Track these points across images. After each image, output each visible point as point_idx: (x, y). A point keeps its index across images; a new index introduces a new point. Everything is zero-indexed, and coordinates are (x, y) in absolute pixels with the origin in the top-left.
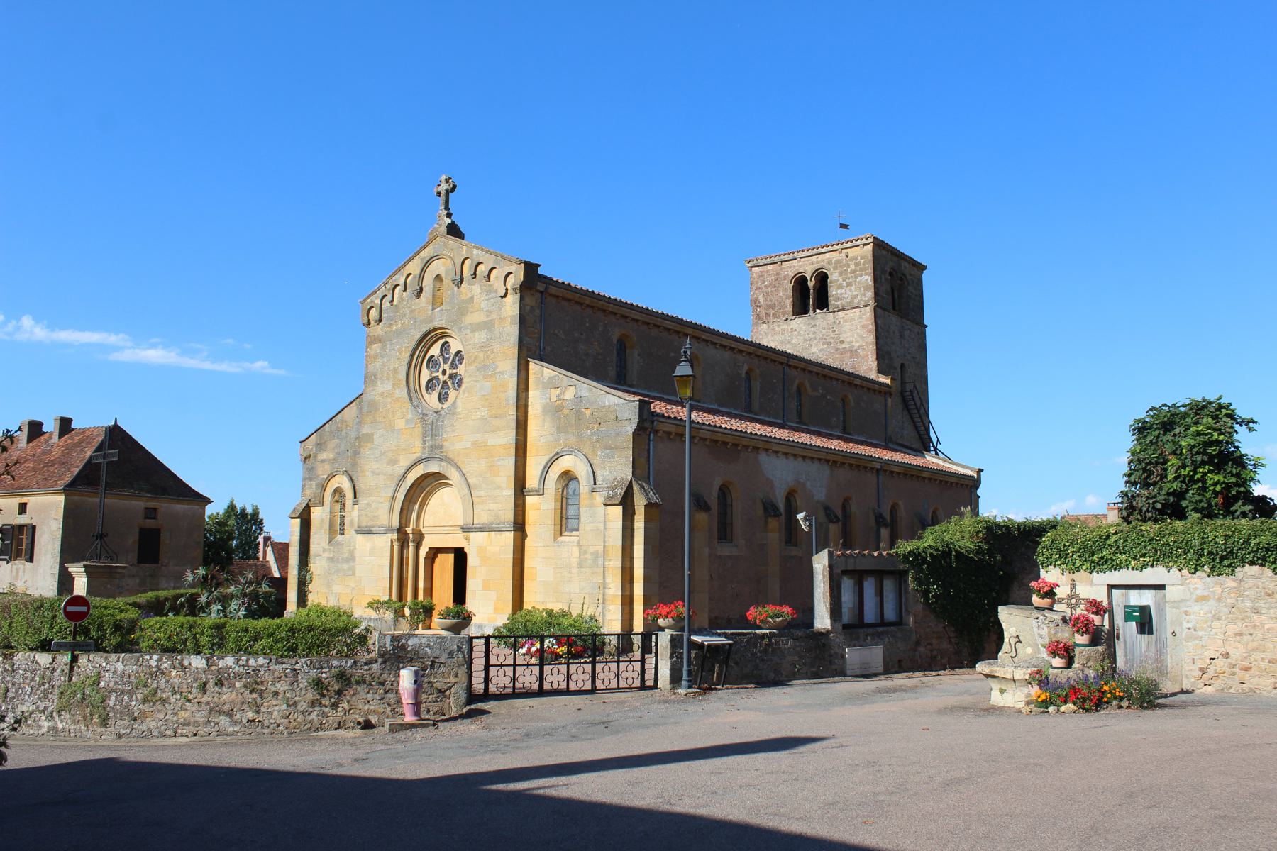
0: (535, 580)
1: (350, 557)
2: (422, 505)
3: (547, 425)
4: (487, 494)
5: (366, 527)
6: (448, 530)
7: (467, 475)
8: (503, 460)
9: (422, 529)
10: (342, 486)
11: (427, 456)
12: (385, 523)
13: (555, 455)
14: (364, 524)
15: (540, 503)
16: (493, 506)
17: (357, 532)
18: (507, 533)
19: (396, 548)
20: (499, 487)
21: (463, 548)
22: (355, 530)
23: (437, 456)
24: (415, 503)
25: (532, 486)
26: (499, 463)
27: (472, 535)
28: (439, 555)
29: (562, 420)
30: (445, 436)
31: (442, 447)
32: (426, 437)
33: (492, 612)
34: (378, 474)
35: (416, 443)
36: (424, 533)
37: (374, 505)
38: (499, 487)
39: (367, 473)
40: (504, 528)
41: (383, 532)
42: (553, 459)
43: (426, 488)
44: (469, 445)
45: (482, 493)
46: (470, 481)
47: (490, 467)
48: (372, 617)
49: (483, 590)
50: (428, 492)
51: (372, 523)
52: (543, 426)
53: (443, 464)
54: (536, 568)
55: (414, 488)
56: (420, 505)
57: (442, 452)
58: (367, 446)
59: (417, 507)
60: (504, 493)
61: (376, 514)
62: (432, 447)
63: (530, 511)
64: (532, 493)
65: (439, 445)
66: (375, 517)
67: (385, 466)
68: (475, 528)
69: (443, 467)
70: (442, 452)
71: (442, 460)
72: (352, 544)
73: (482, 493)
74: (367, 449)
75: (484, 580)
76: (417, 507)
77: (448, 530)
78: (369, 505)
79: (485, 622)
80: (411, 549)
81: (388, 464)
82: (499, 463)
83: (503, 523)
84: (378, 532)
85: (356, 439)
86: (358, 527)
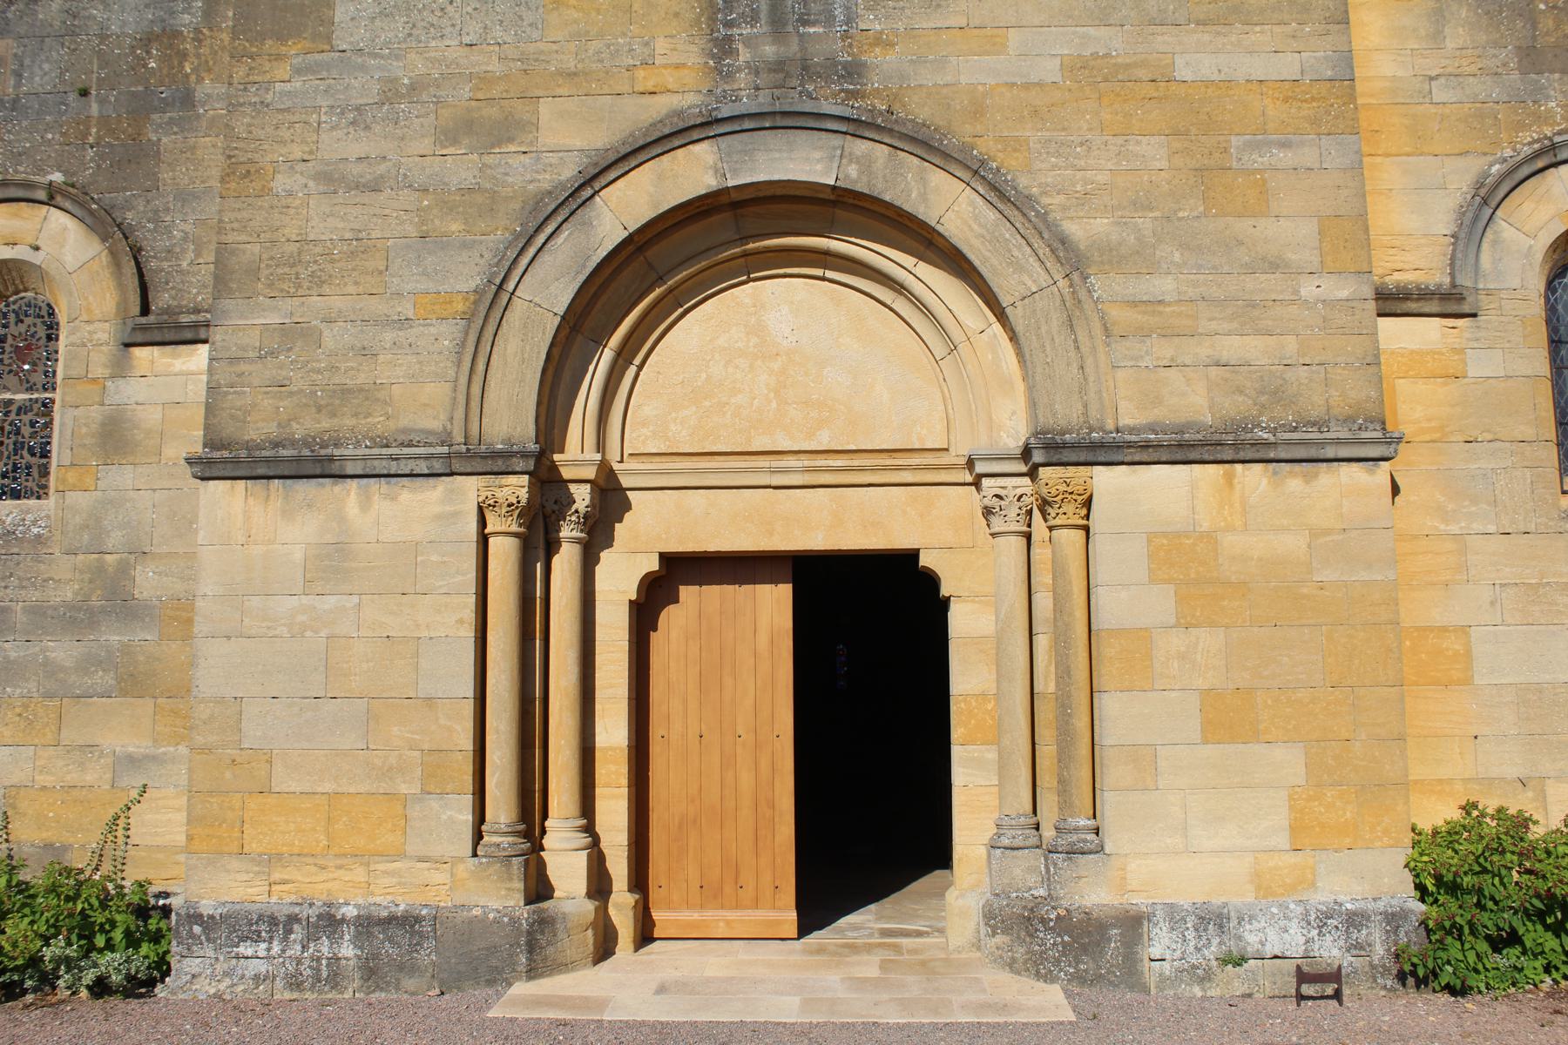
0: (1467, 681)
1: (96, 602)
2: (624, 356)
3: (1457, 36)
4: (1191, 292)
5: (276, 445)
6: (808, 470)
7: (1053, 201)
8: (1284, 145)
9: (616, 466)
10: (36, 258)
11: (746, 104)
12: (436, 425)
13: (1537, 155)
14: (259, 428)
15: (1462, 351)
16: (1233, 347)
17: (208, 468)
18: (1355, 467)
19: (504, 552)
20: (1275, 265)
21: (913, 555)
22: (190, 461)
23: (827, 107)
24: (599, 341)
25: (1397, 276)
26: (1260, 160)
27: (1106, 481)
28: (687, 592)
29: (1547, 23)
30: (870, 22)
31: (854, 71)
32: (729, 24)
33: (1282, 841)
34: (376, 189)
35: (661, 45)
36: (625, 482)
37: (332, 337)
38: (1275, 265)
39: (281, 183)
40: (1338, 442)
41: (422, 467)
42: (1526, 171)
43: (672, 271)
44: (1049, 70)
45: (1164, 286)
46: (1074, 229)
47: (1199, 170)
48: (350, 912)
49: (1205, 742)
50: (670, 291)
51: (326, 424)
52: (1437, 36)
53: (861, 147)
54: (1464, 630)
55: (615, 264)
56: (619, 353)
57: (853, 95)
58: (279, 57)
59: (607, 355)
60: (1308, 289)
61: (362, 379)
62: (779, 66)
63: (1401, 384)
64: (1412, 306)
65: (832, 62)
66: (345, 392)
67: (425, 145)
68: (1146, 446)
69: (866, 164)
70: (853, 95)
71: (857, 127)
72: (115, 539)
73: (1164, 286)
74: (283, 71)
75: (1206, 693)
76: (607, 355)
77: (808, 470)
78: (294, 334)
79: (1238, 896)
80: (565, 562)
81: (448, 136)
82: (1260, 160)
83: (1319, 424)
84: (381, 466)
85: (147, 40)
86: (210, 443)
